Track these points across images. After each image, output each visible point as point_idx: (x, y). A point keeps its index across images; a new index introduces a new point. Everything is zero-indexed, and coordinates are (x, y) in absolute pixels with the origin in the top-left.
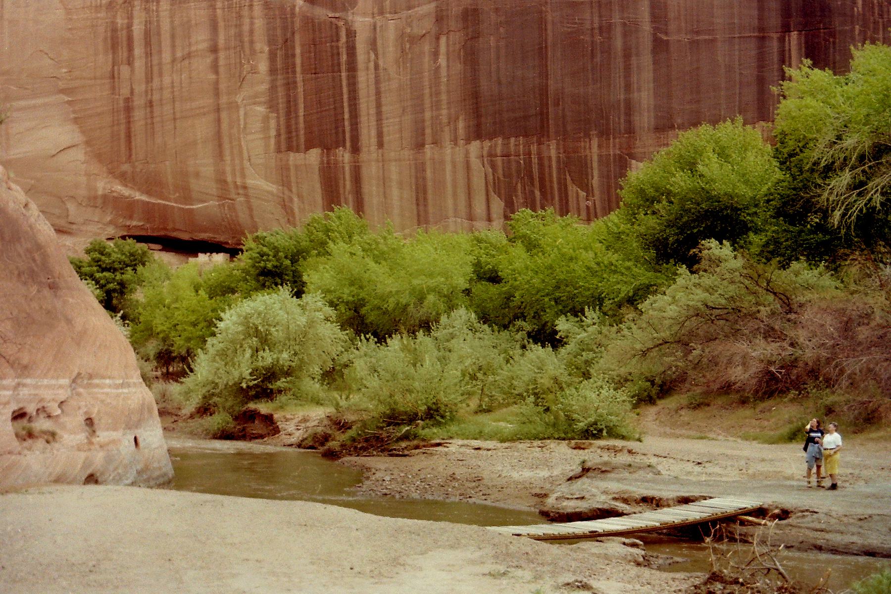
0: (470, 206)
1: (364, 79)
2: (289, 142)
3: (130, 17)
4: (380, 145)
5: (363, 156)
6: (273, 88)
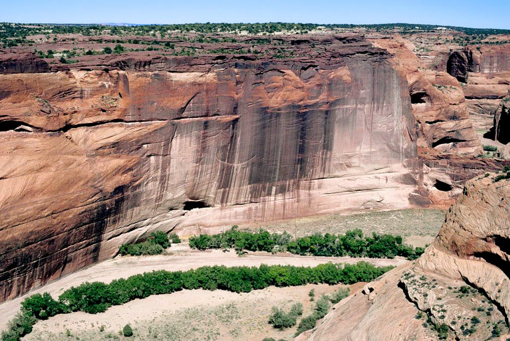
0: (246, 196)
1: (234, 175)
2: (219, 188)
5: (231, 189)
6: (219, 179)
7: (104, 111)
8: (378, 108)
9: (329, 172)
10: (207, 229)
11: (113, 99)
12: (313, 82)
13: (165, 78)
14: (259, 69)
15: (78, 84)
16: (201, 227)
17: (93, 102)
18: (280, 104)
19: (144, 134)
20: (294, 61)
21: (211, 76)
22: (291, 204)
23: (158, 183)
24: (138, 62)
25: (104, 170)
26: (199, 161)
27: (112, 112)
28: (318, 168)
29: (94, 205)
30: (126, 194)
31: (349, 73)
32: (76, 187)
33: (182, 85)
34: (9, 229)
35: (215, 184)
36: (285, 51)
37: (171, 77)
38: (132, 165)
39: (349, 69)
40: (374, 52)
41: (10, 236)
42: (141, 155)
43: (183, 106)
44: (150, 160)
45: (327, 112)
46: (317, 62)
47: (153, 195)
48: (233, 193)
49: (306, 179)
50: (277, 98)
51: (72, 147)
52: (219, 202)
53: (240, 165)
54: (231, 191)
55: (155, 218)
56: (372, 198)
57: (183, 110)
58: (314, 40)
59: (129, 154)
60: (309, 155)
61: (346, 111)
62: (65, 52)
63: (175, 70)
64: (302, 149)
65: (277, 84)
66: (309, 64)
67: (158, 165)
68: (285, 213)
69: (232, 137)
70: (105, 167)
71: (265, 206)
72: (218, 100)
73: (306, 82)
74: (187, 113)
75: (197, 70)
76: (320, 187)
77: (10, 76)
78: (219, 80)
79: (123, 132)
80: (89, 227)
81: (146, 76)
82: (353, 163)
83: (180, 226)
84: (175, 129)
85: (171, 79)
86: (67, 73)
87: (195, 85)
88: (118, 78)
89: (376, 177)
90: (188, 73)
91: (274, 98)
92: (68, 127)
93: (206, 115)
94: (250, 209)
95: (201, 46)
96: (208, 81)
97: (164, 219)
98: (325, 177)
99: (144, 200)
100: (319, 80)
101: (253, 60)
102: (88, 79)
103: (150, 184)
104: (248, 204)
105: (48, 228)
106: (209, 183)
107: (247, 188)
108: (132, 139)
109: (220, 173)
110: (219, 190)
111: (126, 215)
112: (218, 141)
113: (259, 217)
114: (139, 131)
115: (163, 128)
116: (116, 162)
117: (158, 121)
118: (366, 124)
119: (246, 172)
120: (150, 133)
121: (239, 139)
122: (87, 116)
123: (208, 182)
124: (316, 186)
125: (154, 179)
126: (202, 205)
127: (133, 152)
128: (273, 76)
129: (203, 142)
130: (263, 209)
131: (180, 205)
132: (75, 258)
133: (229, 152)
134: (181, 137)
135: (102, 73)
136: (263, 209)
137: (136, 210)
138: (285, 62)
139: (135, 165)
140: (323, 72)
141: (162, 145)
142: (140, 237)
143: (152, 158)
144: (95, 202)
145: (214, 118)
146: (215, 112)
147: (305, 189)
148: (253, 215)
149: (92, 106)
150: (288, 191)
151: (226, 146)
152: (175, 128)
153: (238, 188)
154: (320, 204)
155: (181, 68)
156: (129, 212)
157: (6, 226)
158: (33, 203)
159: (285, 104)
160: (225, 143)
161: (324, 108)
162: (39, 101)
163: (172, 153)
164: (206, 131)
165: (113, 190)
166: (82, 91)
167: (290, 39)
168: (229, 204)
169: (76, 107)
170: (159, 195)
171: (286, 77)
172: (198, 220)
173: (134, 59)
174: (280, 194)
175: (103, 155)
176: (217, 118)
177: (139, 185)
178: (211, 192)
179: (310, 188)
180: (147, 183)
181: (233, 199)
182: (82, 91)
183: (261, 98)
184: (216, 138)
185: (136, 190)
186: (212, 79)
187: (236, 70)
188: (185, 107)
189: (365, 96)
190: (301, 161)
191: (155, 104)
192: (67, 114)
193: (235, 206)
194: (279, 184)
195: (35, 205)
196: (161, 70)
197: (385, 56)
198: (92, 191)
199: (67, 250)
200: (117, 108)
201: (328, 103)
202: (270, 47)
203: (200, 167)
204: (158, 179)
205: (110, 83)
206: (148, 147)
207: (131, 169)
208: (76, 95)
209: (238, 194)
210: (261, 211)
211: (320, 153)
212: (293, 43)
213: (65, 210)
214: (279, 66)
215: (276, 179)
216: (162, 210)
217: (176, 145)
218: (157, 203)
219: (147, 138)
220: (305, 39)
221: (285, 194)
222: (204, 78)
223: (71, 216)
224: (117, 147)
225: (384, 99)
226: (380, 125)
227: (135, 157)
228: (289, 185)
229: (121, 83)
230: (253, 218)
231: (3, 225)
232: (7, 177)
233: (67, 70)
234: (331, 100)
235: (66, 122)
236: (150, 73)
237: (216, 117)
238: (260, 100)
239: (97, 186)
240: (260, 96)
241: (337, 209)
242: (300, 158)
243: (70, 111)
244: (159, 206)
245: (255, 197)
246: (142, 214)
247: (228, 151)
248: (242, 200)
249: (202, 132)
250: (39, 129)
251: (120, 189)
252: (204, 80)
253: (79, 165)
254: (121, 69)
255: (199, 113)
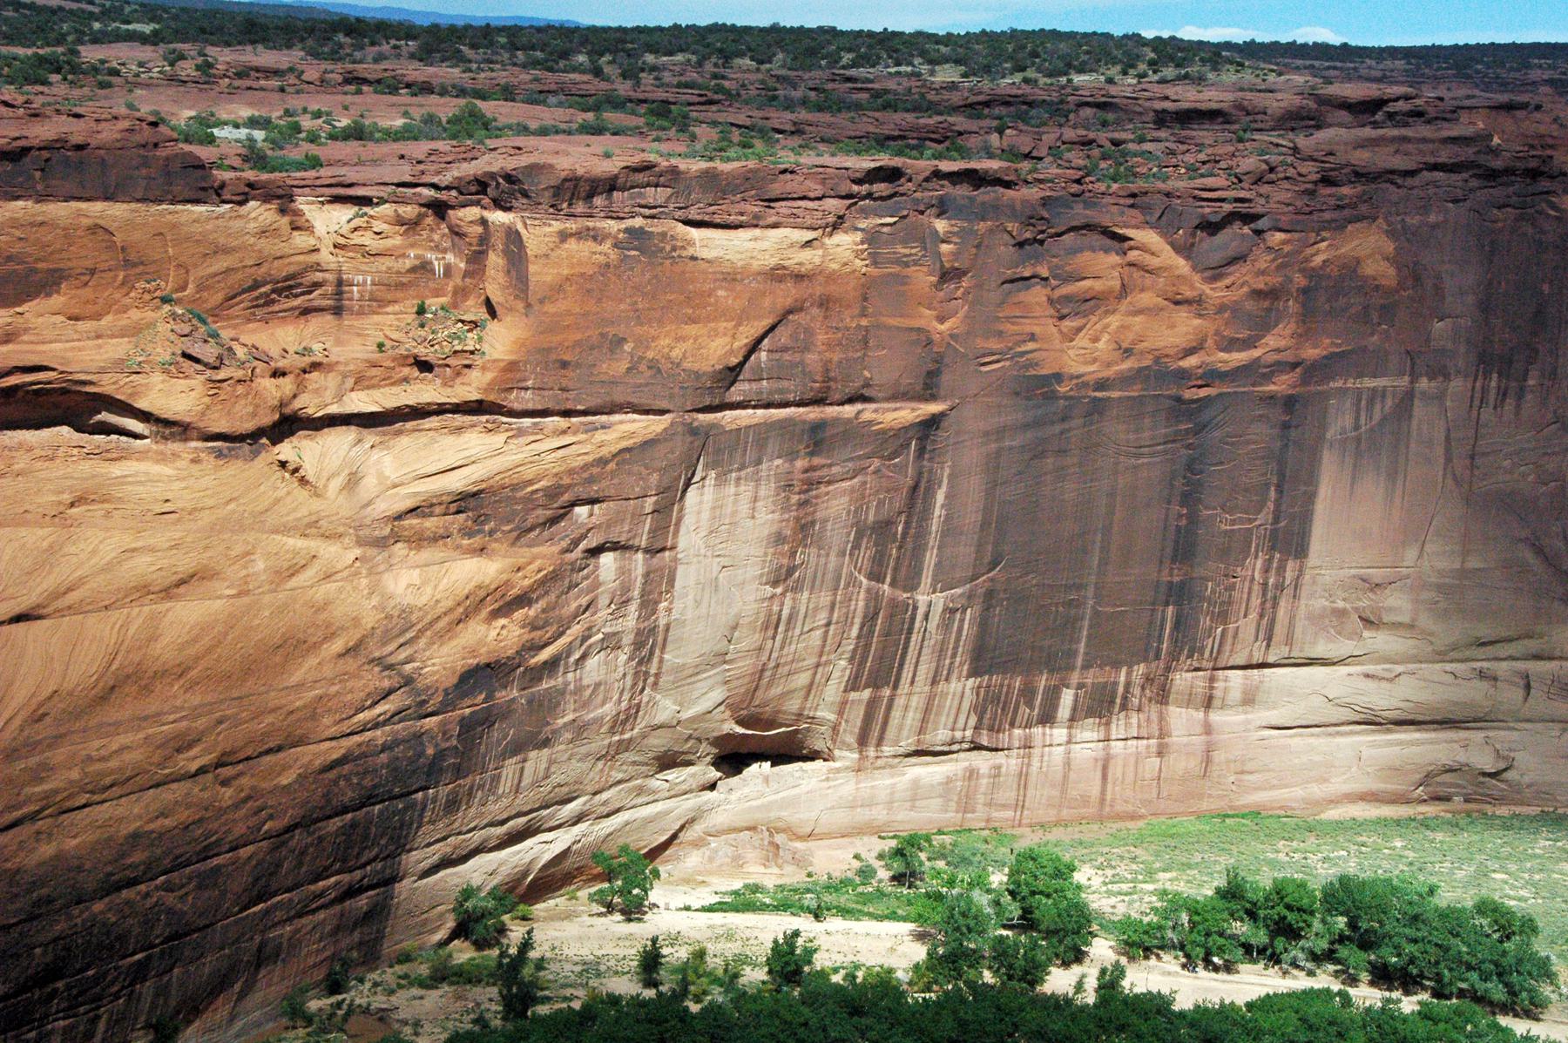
0: (955, 722)
1: (915, 638)
2: (853, 685)
3: (782, 605)
4: (912, 682)
5: (899, 691)
6: (855, 651)
7: (425, 366)
8: (1505, 394)
9: (1289, 640)
10: (798, 845)
11: (463, 322)
12: (1245, 278)
13: (668, 248)
14: (1030, 220)
15: (326, 256)
16: (779, 838)
17: (392, 325)
18: (1109, 365)
19: (580, 461)
20: (1168, 195)
21: (844, 245)
22: (1132, 760)
23: (623, 658)
24: (565, 180)
25: (424, 600)
26: (783, 577)
27: (458, 374)
28: (1247, 626)
29: (379, 736)
30: (503, 696)
31: (1390, 247)
32: (312, 661)
33: (731, 277)
34: (49, 820)
35: (841, 668)
36: (1124, 154)
37: (691, 243)
38: (527, 582)
39: (1391, 234)
40: (1498, 164)
41: (47, 850)
42: (564, 544)
43: (734, 361)
44: (597, 567)
45: (1290, 402)
46: (1262, 201)
47: (603, 703)
48: (906, 708)
49: (1196, 664)
50: (1096, 340)
51: (301, 504)
52: (851, 739)
53: (939, 600)
54: (900, 702)
55: (604, 796)
56: (1462, 757)
57: (732, 373)
58: (1248, 114)
59: (518, 538)
60: (1208, 569)
61: (1371, 402)
62: (253, 123)
63: (706, 218)
64: (1184, 548)
65: (1097, 285)
66: (1227, 207)
67: (626, 589)
68: (1109, 797)
69: (915, 488)
70: (429, 590)
71: (1029, 765)
72: (865, 342)
73: (1214, 279)
74: (746, 386)
75: (795, 222)
76: (1249, 700)
77: (59, 210)
78: (875, 263)
79: (498, 452)
80: (353, 825)
81: (595, 238)
82: (1390, 610)
83: (696, 831)
84: (701, 451)
85: (691, 251)
86: (283, 211)
87: (781, 279)
88: (484, 240)
89: (1482, 675)
90: (757, 232)
91: (1082, 341)
92: (288, 424)
93: (819, 401)
94: (972, 774)
95: (795, 124)
96: (834, 266)
97: (640, 800)
98: (1271, 660)
99: (565, 725)
100: (1263, 273)
101: (1008, 185)
102: (367, 239)
103: (592, 662)
104: (962, 755)
105: (201, 820)
106: (818, 666)
107: (962, 688)
108: (530, 482)
109: (861, 629)
110: (853, 695)
111: (496, 779)
112: (860, 498)
113: (1004, 806)
114: (561, 452)
115: (648, 444)
116: (471, 571)
117: (636, 416)
118: (1448, 459)
119: (960, 629)
120: (602, 462)
121: (940, 497)
122: (360, 382)
123: (814, 660)
124: (1235, 695)
125: (611, 643)
126: (787, 752)
127: (532, 535)
128: (1081, 250)
129: (802, 504)
130: (1023, 778)
131: (704, 748)
132: (294, 943)
133: (900, 548)
134: (721, 481)
135: (421, 217)
136: (1023, 778)
137: (537, 760)
138: (1134, 195)
139: (542, 582)
140: (1285, 242)
141: (648, 509)
142: (546, 867)
143: (607, 559)
144: (385, 723)
145: (849, 410)
146: (854, 386)
147: (1189, 702)
148: (981, 799)
149: (380, 346)
150: (1124, 707)
151: (889, 523)
152: (698, 443)
153: (927, 688)
154: (1248, 767)
155: (730, 209)
156: (510, 768)
157: (33, 808)
158: (145, 718)
159: (1126, 365)
160: (885, 512)
161: (1281, 385)
162: (174, 316)
163: (682, 543)
164: (817, 461)
165: (455, 680)
166: (340, 283)
167: (1148, 104)
168: (887, 750)
169: (317, 347)
170: (624, 705)
171: (1133, 255)
172: (767, 807)
173: (551, 166)
174: (1091, 720)
175: (419, 541)
176: (859, 412)
177: (552, 665)
178: (828, 701)
179: (1208, 703)
180: (584, 657)
181: (905, 733)
182: (340, 283)
183: (1032, 337)
184: (853, 490)
185: (540, 679)
186: (849, 255)
187: (941, 225)
188: (742, 364)
189: (1449, 346)
190: (1180, 594)
191: (628, 347)
192: (284, 374)
193: (914, 760)
194: (1089, 681)
195: (150, 731)
196: (653, 217)
197: (1545, 184)
198: (378, 680)
199: (267, 912)
200: (478, 360)
201: (1294, 366)
202: (1069, 134)
203: (788, 602)
204: (627, 639)
205: (450, 257)
206: (591, 515)
207: (523, 600)
208: (316, 298)
209: (927, 711)
210: (1012, 782)
211: (1255, 566)
212: (1162, 119)
213: (269, 751)
214: (1108, 216)
215: (1079, 662)
216: (634, 763)
217: (699, 513)
218: (617, 738)
219: (591, 480)
220: (1214, 106)
221: (1108, 724)
222: (820, 252)
223: (286, 780)
224: (476, 511)
225: (1530, 361)
226: (1507, 463)
227: (541, 556)
228: (1128, 685)
229: (495, 260)
230: (979, 807)
231: (25, 803)
232: (45, 611)
233: (282, 199)
234: (1311, 353)
235: (282, 405)
236: (613, 226)
237: (859, 406)
238: (1031, 346)
239: (392, 660)
240: (1028, 329)
241: (1317, 791)
242: (1176, 579)
243: (293, 362)
244: (624, 746)
245: (991, 729)
246: (556, 778)
247: (891, 543)
248: (939, 736)
249: (800, 464)
250: (174, 429)
251: (483, 675)
252: (817, 261)
253: (328, 577)
254: (499, 204)
255: (792, 389)
